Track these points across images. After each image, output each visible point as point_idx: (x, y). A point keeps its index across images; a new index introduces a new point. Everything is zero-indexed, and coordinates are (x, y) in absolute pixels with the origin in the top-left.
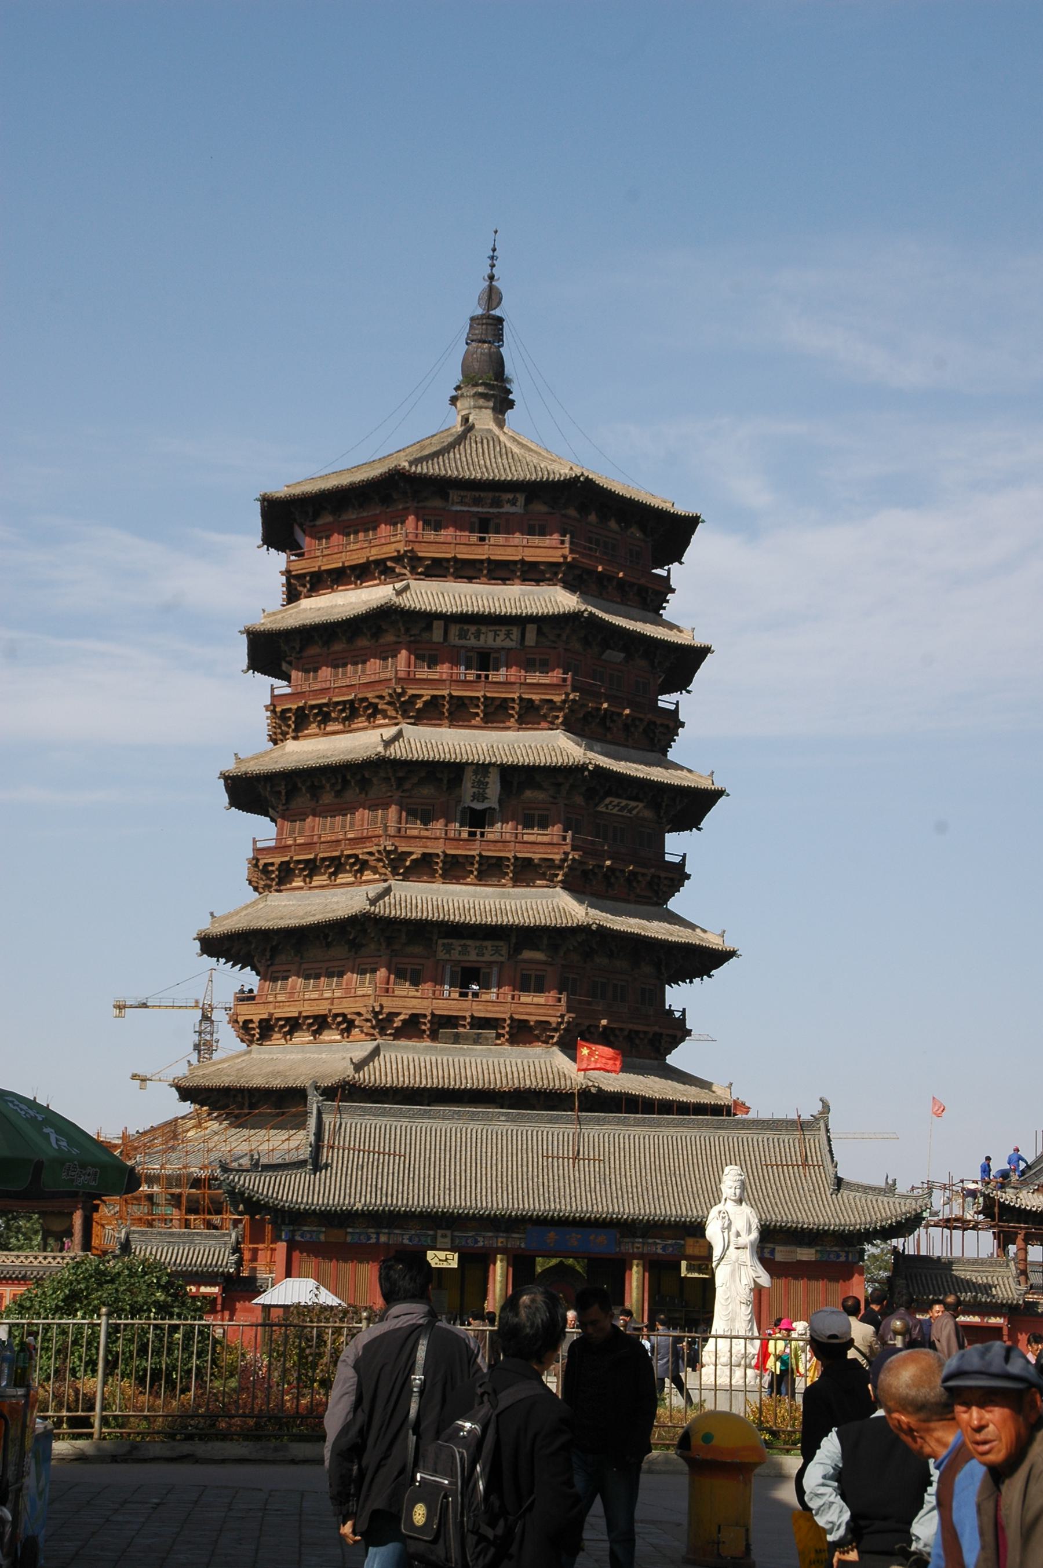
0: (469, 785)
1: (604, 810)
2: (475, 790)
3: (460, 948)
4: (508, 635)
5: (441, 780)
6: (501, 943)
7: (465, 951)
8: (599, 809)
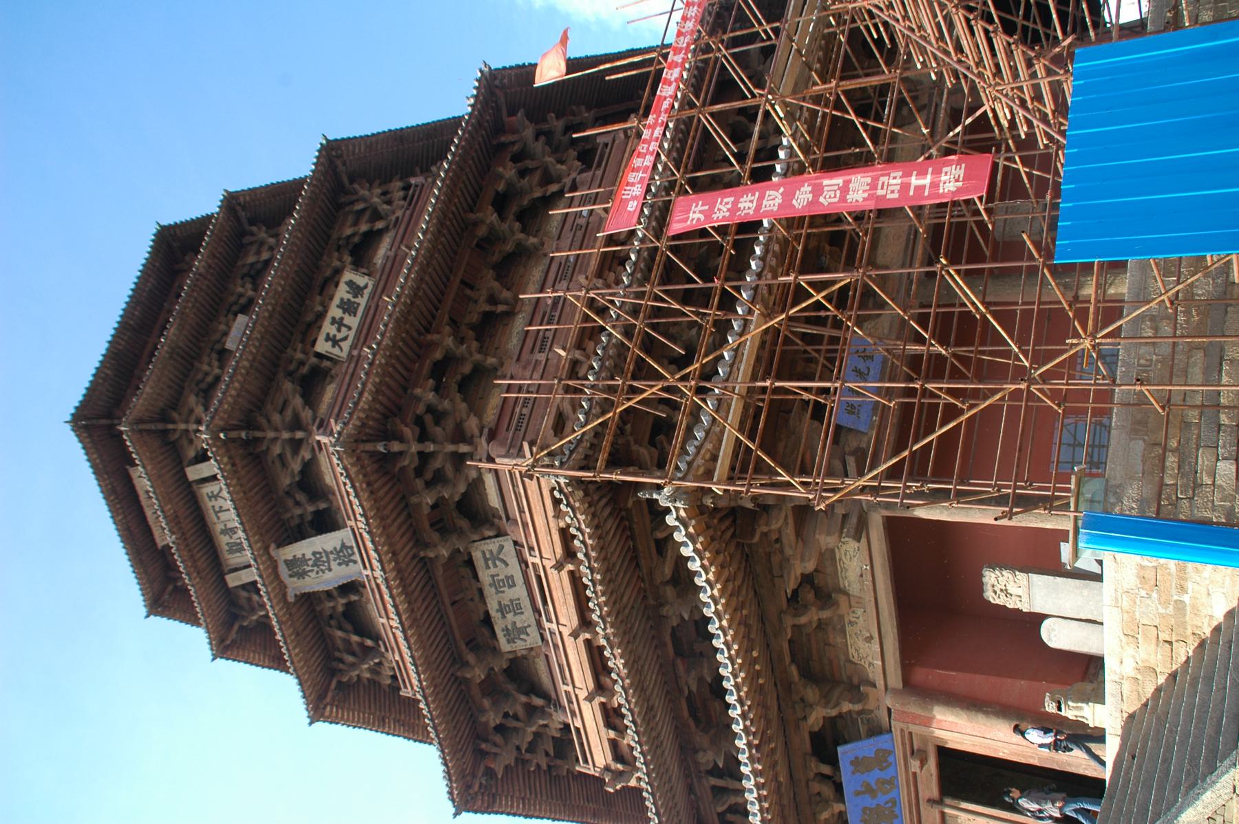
0: (328, 575)
1: (346, 345)
2: (334, 565)
3: (510, 616)
4: (216, 497)
5: (349, 605)
6: (477, 556)
7: (516, 607)
8: (344, 355)
